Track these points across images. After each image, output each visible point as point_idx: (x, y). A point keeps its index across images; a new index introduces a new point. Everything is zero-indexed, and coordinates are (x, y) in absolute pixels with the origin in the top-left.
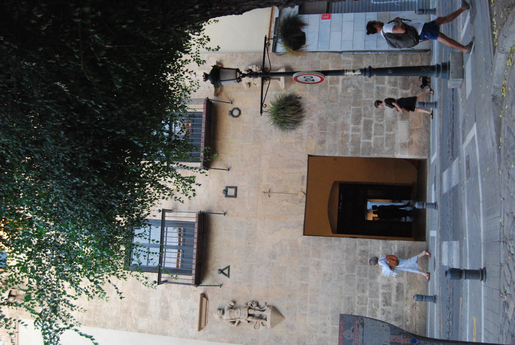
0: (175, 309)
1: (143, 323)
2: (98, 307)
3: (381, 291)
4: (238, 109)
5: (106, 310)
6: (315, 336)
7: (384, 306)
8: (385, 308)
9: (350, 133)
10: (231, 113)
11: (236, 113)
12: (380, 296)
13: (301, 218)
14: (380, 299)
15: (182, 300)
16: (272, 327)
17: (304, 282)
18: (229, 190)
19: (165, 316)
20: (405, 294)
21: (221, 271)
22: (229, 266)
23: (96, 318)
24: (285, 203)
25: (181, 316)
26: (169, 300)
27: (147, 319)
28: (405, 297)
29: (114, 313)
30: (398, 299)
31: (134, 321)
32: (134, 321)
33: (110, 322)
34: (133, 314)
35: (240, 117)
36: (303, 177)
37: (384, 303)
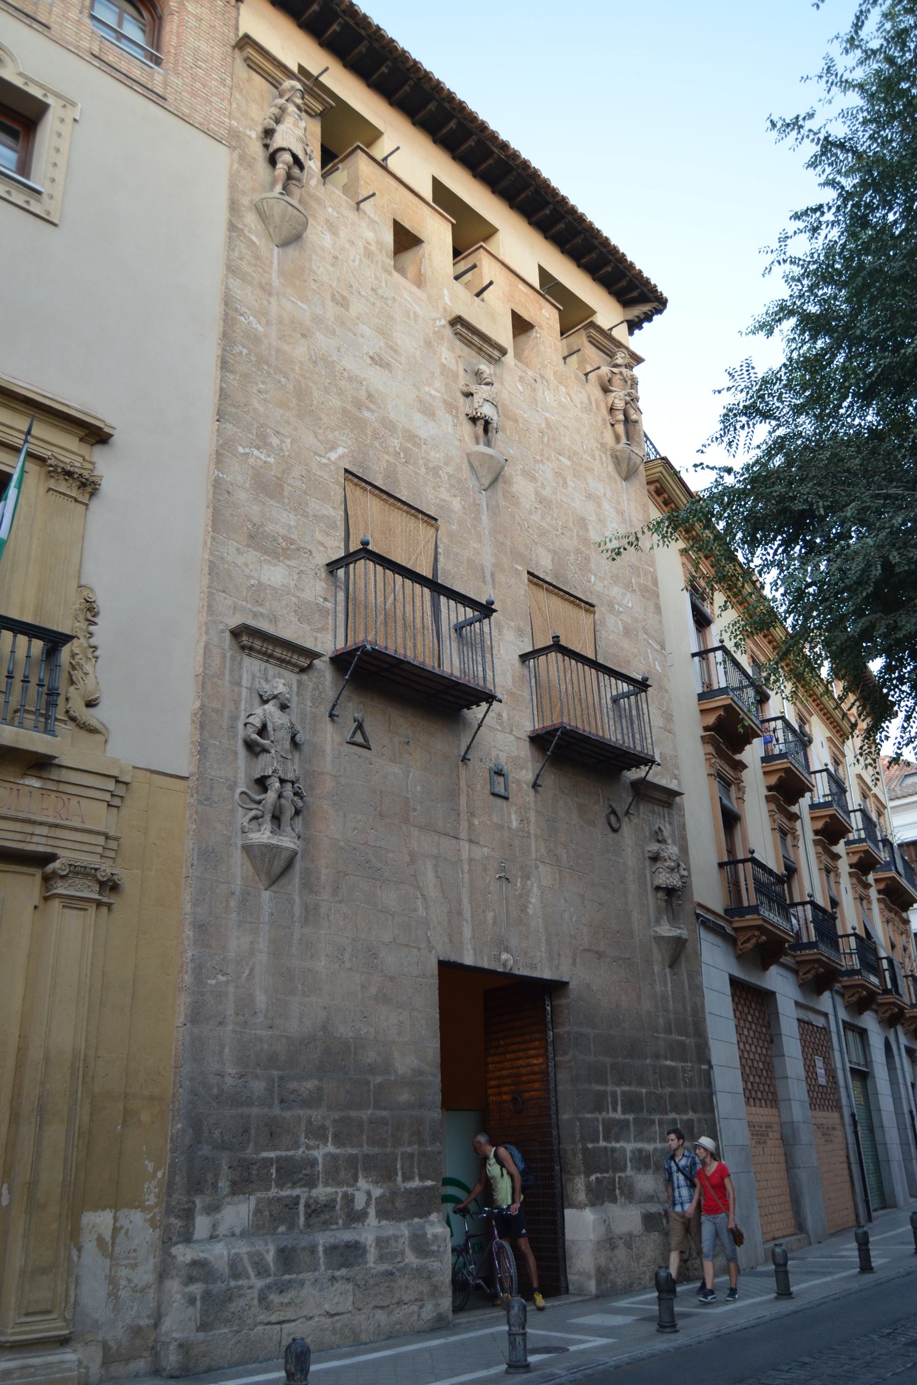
0: (275, 575)
1: (236, 474)
2: (265, 367)
3: (341, 1191)
4: (620, 827)
5: (262, 386)
6: (227, 982)
7: (307, 1206)
8: (301, 1208)
9: (610, 1088)
10: (614, 812)
11: (613, 819)
12: (329, 1190)
13: (468, 960)
14: (322, 1192)
15: (294, 599)
16: (248, 849)
17: (347, 956)
18: (501, 779)
19: (257, 539)
20: (344, 1271)
21: (360, 727)
22: (370, 749)
23: (245, 351)
24: (490, 915)
25: (260, 584)
26: (291, 563)
27: (248, 485)
28: (337, 1274)
29: (256, 404)
30: (331, 1250)
31: (241, 450)
32: (241, 450)
33: (235, 383)
34: (256, 452)
35: (609, 829)
36: (533, 967)
37: (313, 1207)
